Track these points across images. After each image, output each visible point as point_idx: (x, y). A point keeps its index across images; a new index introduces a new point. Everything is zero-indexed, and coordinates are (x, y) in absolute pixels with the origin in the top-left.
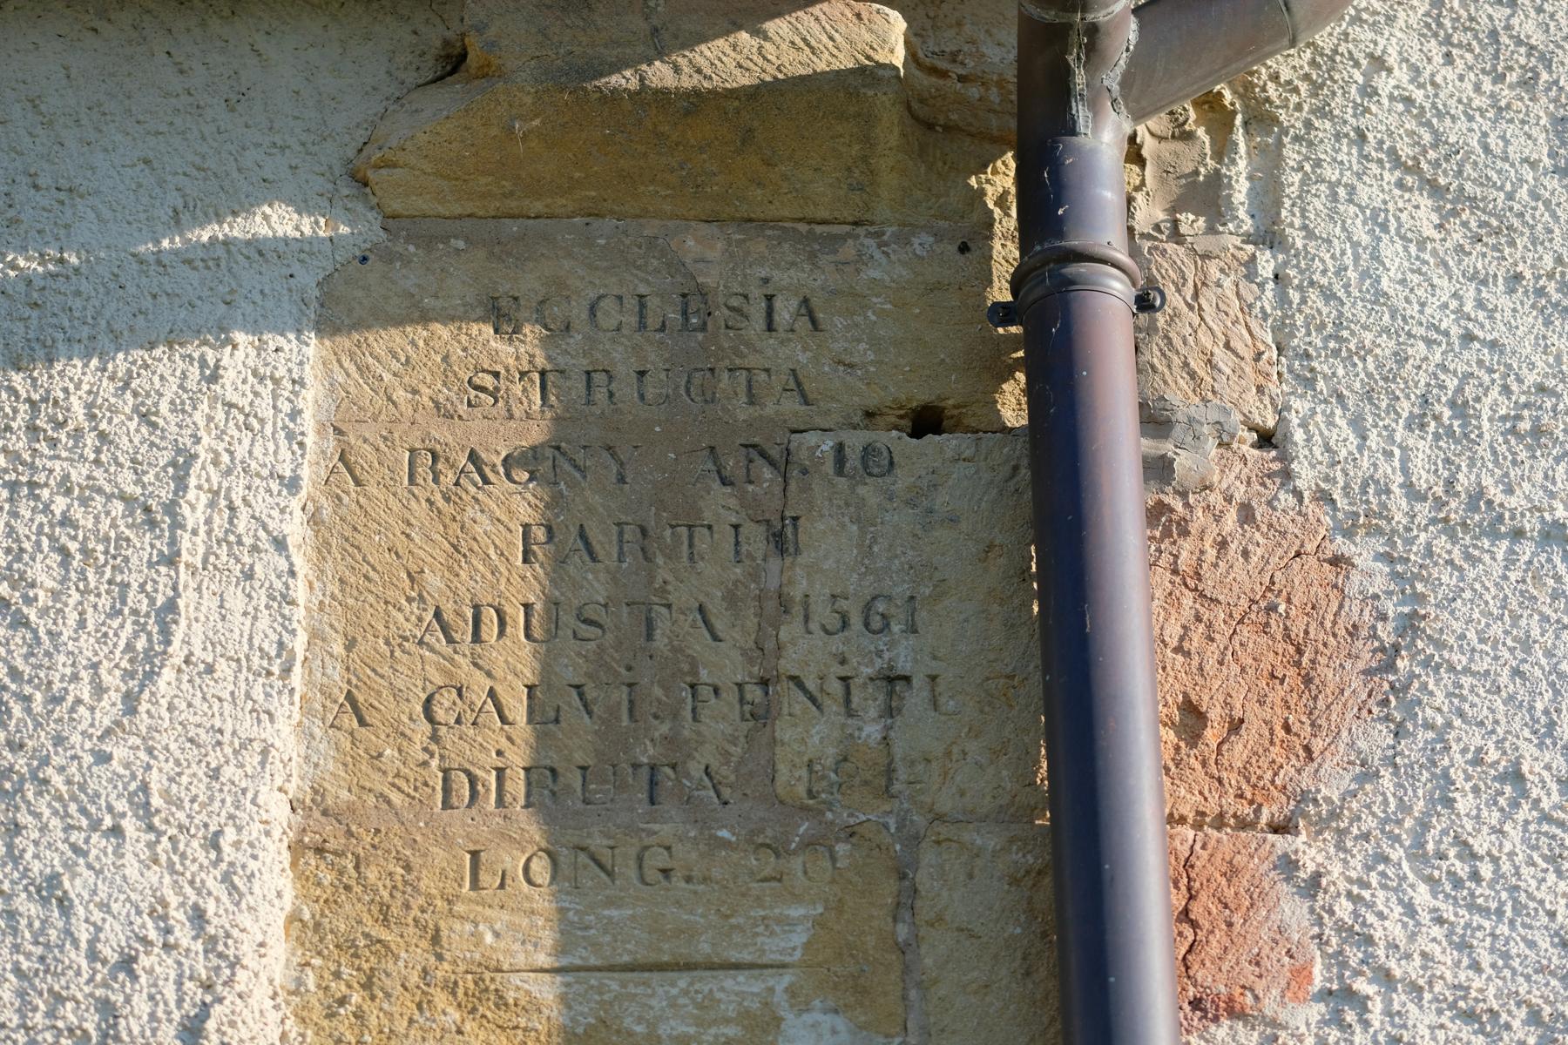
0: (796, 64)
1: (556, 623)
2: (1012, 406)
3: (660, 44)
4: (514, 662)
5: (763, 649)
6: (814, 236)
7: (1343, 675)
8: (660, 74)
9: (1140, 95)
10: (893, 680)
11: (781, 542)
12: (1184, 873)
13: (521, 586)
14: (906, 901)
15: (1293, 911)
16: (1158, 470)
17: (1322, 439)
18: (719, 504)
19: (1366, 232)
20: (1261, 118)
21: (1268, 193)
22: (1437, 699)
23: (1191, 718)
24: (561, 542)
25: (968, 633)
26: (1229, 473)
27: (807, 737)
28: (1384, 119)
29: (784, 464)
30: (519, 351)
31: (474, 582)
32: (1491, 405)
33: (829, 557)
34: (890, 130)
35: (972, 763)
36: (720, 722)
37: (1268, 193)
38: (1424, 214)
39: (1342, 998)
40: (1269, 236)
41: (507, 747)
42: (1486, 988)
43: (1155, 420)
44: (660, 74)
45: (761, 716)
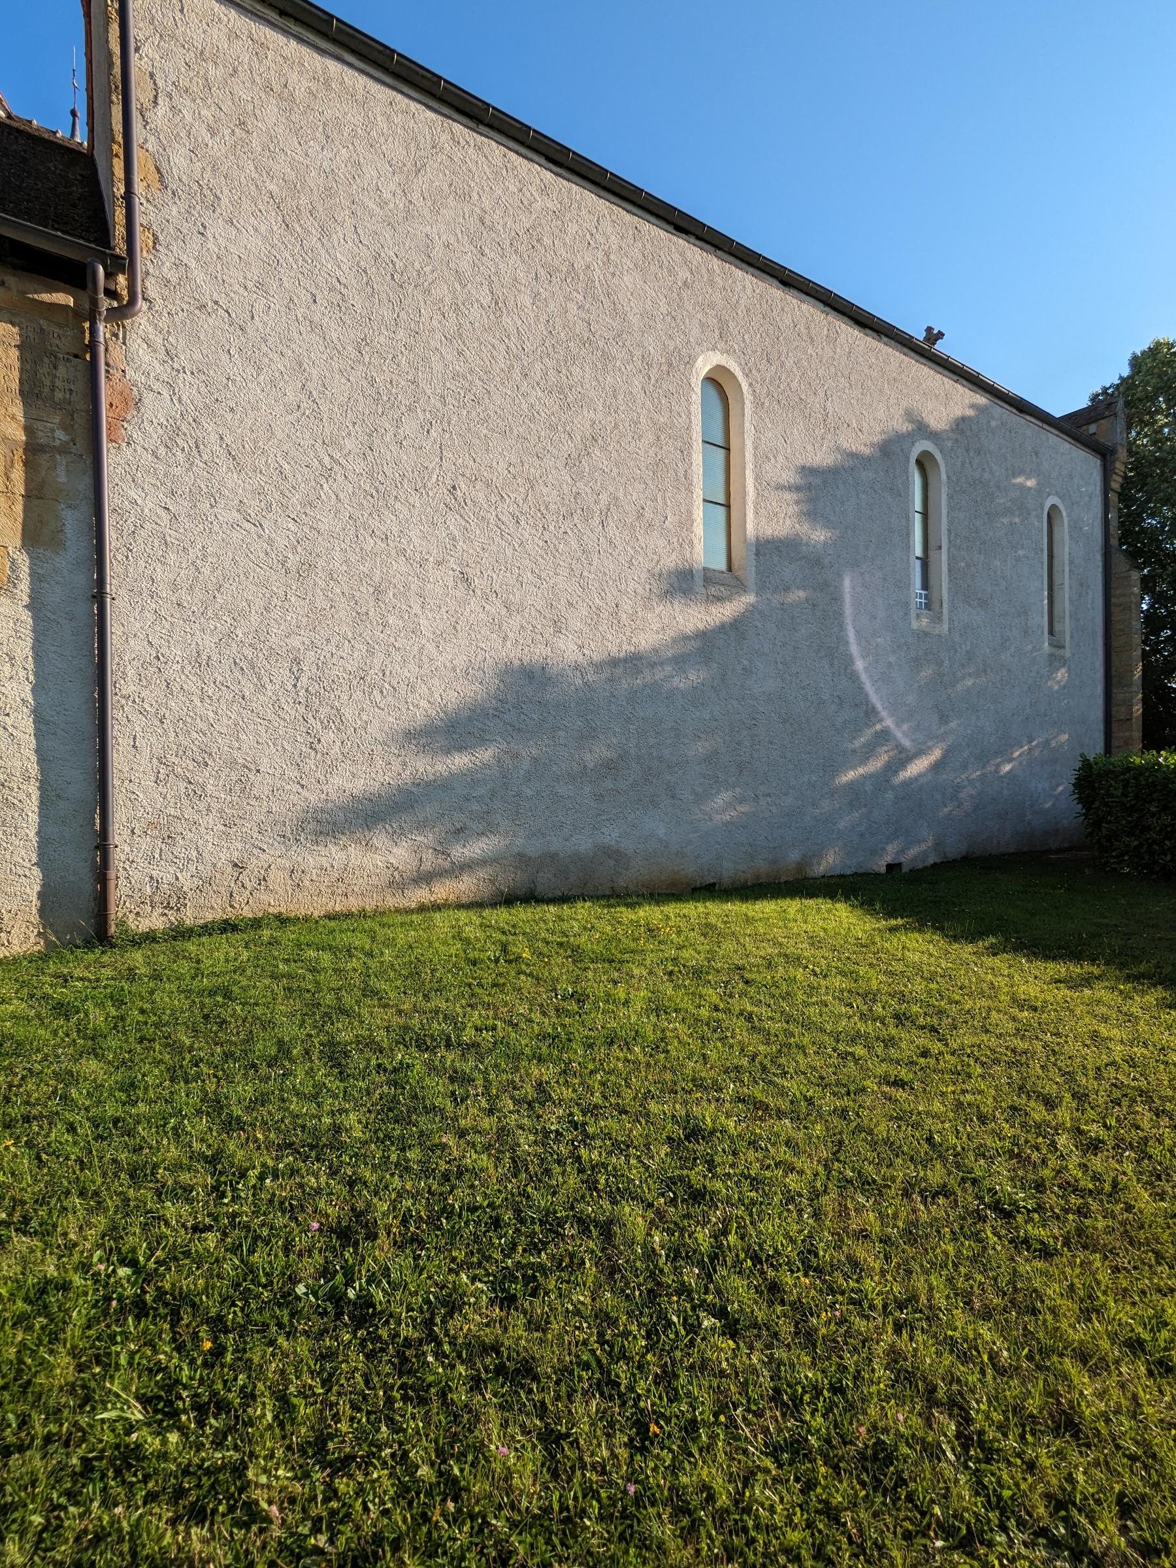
0: (57, 301)
1: (22, 371)
2: (88, 357)
3: (36, 292)
4: (16, 374)
5: (53, 382)
6: (60, 326)
7: (131, 404)
8: (36, 296)
9: (106, 320)
10: (71, 390)
11: (55, 368)
12: (108, 423)
13: (17, 364)
14: (73, 419)
15: (123, 431)
16: (107, 371)
17: (130, 373)
18: (46, 360)
19: (136, 344)
20: (124, 327)
21: (124, 338)
22: (143, 410)
23: (111, 405)
24: (22, 359)
25: (80, 386)
26: (118, 375)
27: (59, 395)
28: (140, 332)
29: (55, 357)
30: (16, 330)
31: (9, 361)
32: (152, 374)
33: (62, 371)
34: (71, 315)
35: (80, 403)
36: (47, 390)
37: (124, 338)
38: (145, 346)
39: (128, 443)
40: (124, 343)
41: (15, 386)
42: (146, 446)
43: (107, 364)
44: (36, 296)
45: (53, 391)
